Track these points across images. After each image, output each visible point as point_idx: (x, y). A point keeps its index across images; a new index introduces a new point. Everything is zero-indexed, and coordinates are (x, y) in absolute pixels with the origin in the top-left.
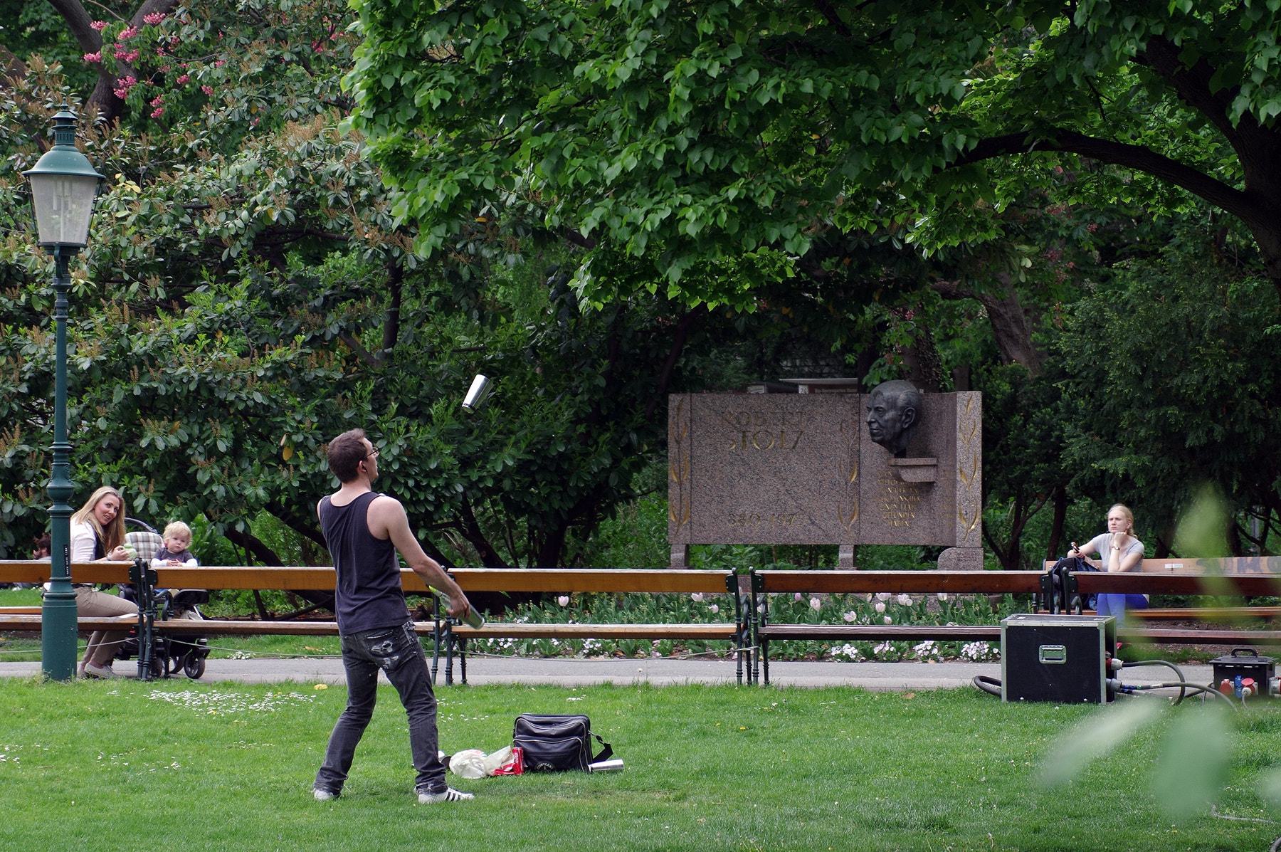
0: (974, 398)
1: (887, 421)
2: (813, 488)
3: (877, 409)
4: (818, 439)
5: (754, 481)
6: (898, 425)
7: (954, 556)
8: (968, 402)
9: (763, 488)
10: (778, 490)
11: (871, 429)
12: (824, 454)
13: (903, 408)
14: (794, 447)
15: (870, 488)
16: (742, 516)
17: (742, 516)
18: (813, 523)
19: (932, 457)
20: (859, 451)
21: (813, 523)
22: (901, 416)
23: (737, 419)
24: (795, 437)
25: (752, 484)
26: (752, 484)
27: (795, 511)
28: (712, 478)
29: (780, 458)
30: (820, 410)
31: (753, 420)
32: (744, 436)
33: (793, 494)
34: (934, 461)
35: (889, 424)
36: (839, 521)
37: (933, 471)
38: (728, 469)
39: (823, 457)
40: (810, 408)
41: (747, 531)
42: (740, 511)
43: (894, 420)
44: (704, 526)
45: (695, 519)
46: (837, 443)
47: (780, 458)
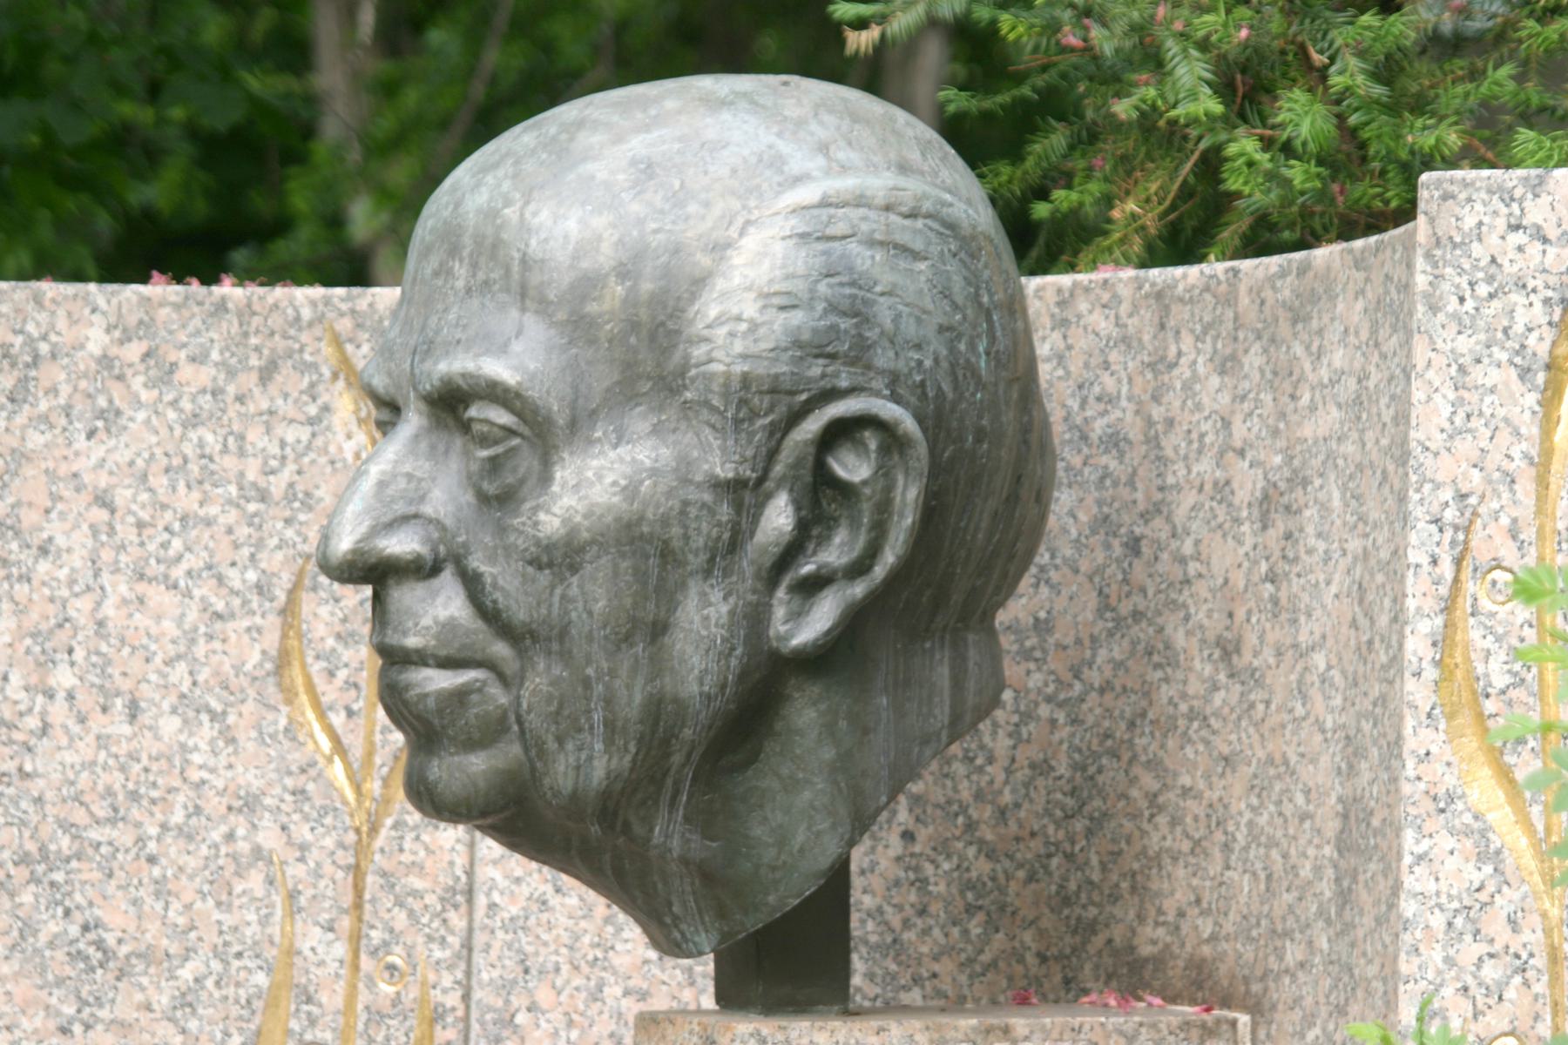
11: (394, 658)
12: (116, 917)
30: (89, 456)
46: (249, 804)
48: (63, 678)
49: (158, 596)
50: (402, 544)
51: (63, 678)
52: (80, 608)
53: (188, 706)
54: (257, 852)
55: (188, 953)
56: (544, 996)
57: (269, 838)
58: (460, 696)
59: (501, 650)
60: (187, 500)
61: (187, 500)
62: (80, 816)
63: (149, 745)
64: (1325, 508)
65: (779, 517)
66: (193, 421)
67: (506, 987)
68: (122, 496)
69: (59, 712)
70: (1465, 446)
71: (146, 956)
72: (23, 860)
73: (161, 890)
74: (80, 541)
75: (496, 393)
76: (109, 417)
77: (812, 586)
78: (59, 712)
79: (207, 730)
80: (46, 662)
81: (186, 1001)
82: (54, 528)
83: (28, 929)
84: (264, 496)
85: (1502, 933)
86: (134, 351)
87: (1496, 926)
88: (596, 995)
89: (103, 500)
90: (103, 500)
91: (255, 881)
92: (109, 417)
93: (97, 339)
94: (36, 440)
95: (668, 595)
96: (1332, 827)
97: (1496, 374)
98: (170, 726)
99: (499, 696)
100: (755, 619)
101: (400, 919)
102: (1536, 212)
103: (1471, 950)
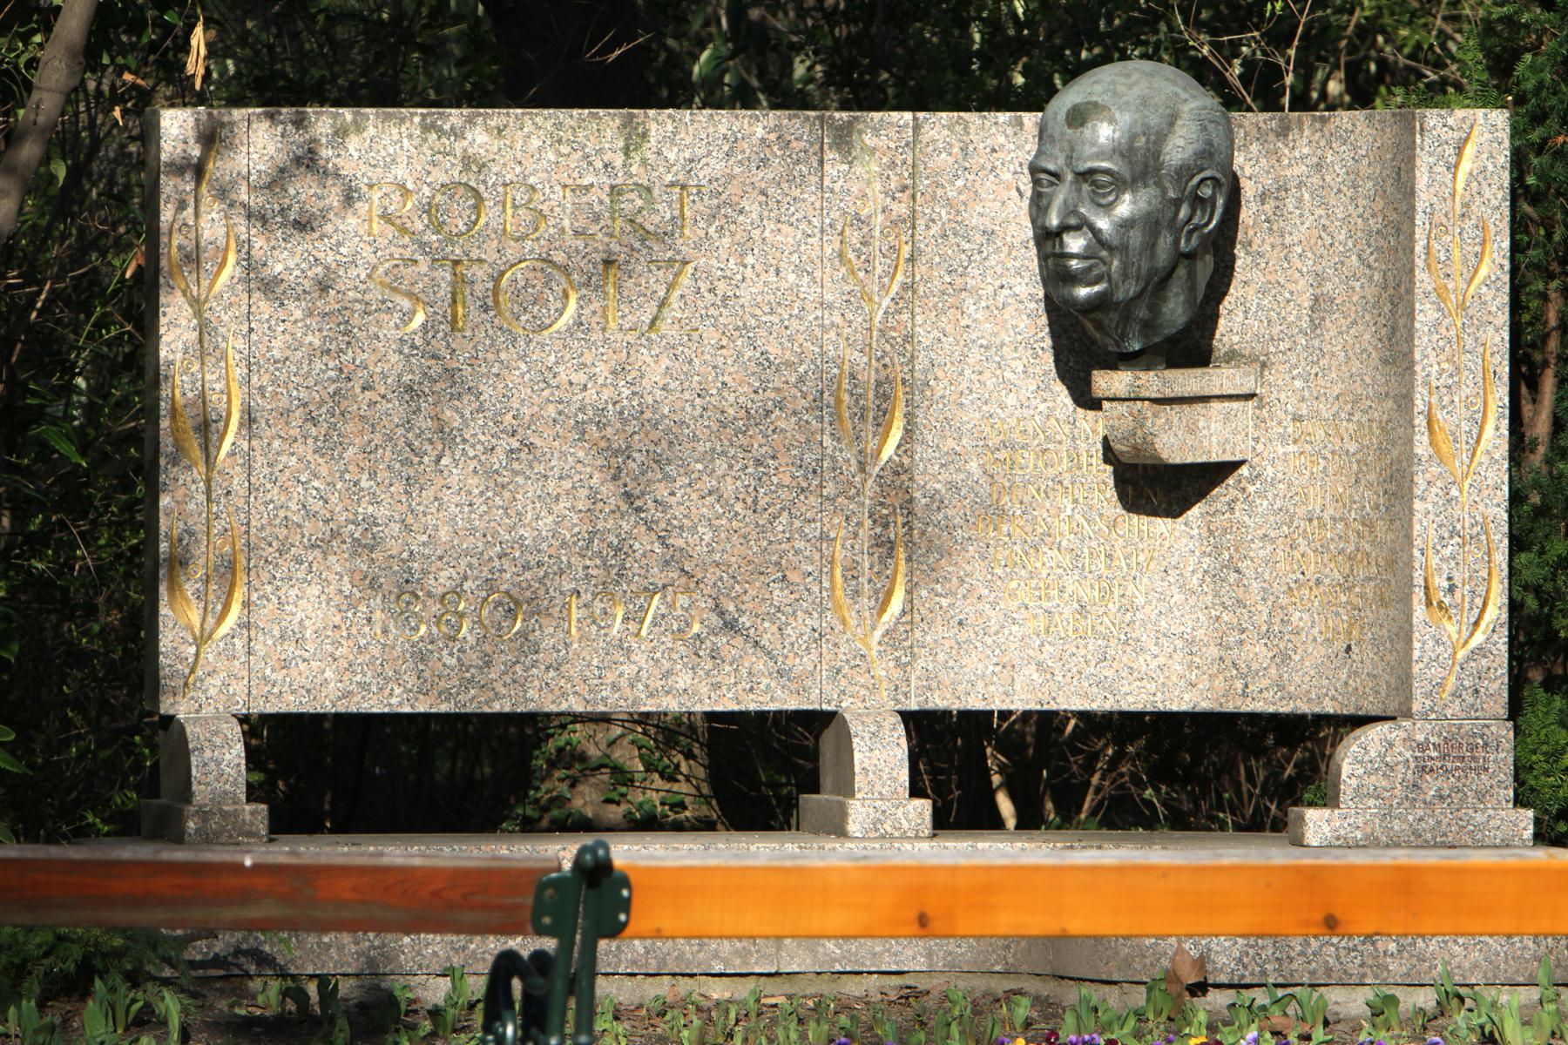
20: (909, 338)
35: (1136, 238)
48: (750, 260)
49: (785, 228)
50: (1073, 221)
53: (800, 270)
54: (833, 324)
55: (801, 362)
56: (940, 375)
57: (837, 319)
59: (1104, 253)
62: (758, 312)
63: (784, 285)
66: (798, 162)
67: (925, 371)
68: (771, 191)
69: (749, 272)
70: (1432, 190)
71: (789, 364)
72: (737, 329)
75: (1107, 172)
79: (806, 279)
83: (740, 354)
84: (832, 191)
85: (1443, 331)
86: (773, 136)
88: (961, 374)
89: (763, 193)
91: (832, 335)
94: (737, 170)
98: (792, 277)
101: (888, 347)
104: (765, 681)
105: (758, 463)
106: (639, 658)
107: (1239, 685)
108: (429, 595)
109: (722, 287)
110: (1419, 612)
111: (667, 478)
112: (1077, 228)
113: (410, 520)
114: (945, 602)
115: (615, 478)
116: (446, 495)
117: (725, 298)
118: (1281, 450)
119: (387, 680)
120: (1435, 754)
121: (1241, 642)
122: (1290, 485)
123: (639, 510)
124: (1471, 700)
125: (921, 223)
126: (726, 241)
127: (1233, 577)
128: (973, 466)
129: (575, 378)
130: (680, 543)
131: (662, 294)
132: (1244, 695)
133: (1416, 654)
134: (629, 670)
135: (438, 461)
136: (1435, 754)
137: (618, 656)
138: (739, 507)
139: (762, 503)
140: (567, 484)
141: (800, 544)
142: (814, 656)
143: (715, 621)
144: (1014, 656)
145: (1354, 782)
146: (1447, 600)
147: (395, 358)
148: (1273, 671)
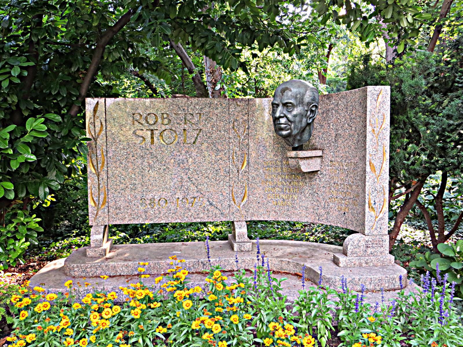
0: (383, 92)
1: (295, 116)
2: (210, 176)
3: (285, 105)
4: (214, 136)
5: (162, 170)
6: (304, 120)
7: (363, 243)
8: (378, 96)
9: (169, 177)
10: (182, 178)
12: (219, 148)
13: (309, 104)
14: (194, 143)
15: (257, 175)
16: (152, 200)
17: (152, 200)
18: (211, 204)
19: (316, 149)
20: (248, 144)
21: (211, 204)
22: (307, 111)
23: (146, 119)
24: (195, 133)
25: (160, 174)
26: (160, 174)
27: (196, 195)
28: (126, 168)
29: (183, 152)
30: (216, 111)
31: (160, 120)
32: (152, 134)
33: (194, 181)
34: (319, 153)
35: (297, 119)
36: (232, 202)
37: (319, 160)
38: (140, 161)
39: (218, 150)
40: (207, 109)
41: (157, 212)
42: (150, 196)
43: (302, 115)
44: (120, 209)
45: (111, 204)
47: (183, 152)
48: (214, 129)
49: (222, 122)
50: (282, 115)
51: (214, 129)
52: (215, 123)
53: (225, 131)
57: (232, 141)
58: (286, 127)
59: (289, 123)
60: (224, 115)
61: (224, 115)
64: (332, 113)
65: (309, 113)
69: (214, 131)
71: (222, 150)
73: (223, 145)
74: (215, 118)
75: (290, 103)
76: (217, 108)
77: (310, 118)
78: (214, 131)
80: (213, 128)
81: (225, 154)
82: (213, 117)
83: (212, 148)
87: (373, 140)
89: (217, 115)
90: (217, 115)
91: (231, 144)
92: (217, 108)
93: (216, 102)
95: (302, 119)
96: (334, 136)
97: (373, 101)
99: (289, 127)
100: (307, 120)
102: (376, 89)
103: (371, 142)
104: (218, 215)
105: (216, 171)
106: (192, 211)
107: (317, 218)
108: (147, 199)
109: (208, 134)
110: (367, 209)
111: (197, 174)
112: (283, 117)
113: (143, 184)
114: (255, 199)
115: (186, 174)
116: (150, 178)
117: (209, 137)
118: (327, 168)
119: (139, 217)
120: (370, 243)
121: (318, 209)
122: (330, 176)
123: (192, 181)
124: (379, 230)
125: (250, 121)
126: (209, 125)
127: (316, 195)
128: (261, 171)
129: (177, 154)
130: (200, 187)
131: (196, 136)
132: (319, 220)
133: (366, 220)
134: (190, 214)
135: (149, 171)
136: (370, 243)
137: (187, 211)
138: (212, 180)
139: (217, 179)
140: (176, 176)
141: (225, 187)
142: (229, 210)
143: (208, 203)
144: (269, 209)
145: (351, 250)
146: (374, 206)
147: (139, 150)
148: (325, 215)
